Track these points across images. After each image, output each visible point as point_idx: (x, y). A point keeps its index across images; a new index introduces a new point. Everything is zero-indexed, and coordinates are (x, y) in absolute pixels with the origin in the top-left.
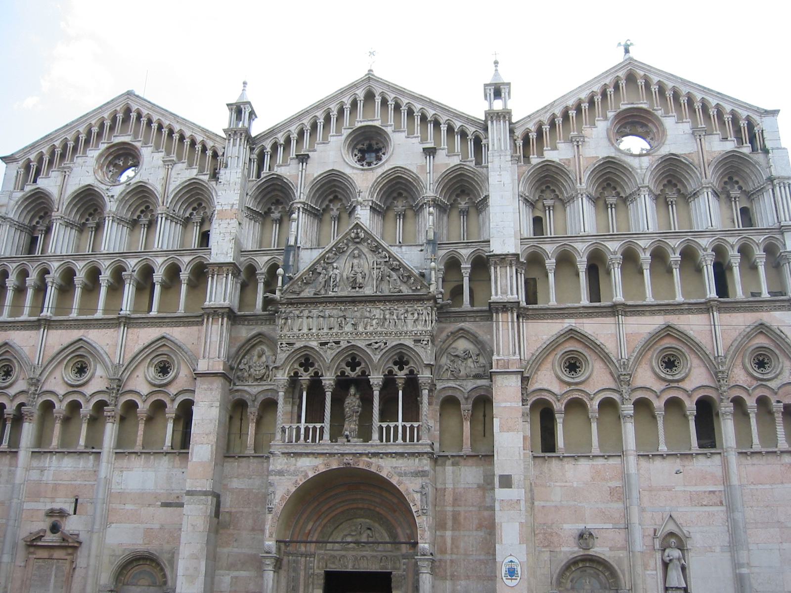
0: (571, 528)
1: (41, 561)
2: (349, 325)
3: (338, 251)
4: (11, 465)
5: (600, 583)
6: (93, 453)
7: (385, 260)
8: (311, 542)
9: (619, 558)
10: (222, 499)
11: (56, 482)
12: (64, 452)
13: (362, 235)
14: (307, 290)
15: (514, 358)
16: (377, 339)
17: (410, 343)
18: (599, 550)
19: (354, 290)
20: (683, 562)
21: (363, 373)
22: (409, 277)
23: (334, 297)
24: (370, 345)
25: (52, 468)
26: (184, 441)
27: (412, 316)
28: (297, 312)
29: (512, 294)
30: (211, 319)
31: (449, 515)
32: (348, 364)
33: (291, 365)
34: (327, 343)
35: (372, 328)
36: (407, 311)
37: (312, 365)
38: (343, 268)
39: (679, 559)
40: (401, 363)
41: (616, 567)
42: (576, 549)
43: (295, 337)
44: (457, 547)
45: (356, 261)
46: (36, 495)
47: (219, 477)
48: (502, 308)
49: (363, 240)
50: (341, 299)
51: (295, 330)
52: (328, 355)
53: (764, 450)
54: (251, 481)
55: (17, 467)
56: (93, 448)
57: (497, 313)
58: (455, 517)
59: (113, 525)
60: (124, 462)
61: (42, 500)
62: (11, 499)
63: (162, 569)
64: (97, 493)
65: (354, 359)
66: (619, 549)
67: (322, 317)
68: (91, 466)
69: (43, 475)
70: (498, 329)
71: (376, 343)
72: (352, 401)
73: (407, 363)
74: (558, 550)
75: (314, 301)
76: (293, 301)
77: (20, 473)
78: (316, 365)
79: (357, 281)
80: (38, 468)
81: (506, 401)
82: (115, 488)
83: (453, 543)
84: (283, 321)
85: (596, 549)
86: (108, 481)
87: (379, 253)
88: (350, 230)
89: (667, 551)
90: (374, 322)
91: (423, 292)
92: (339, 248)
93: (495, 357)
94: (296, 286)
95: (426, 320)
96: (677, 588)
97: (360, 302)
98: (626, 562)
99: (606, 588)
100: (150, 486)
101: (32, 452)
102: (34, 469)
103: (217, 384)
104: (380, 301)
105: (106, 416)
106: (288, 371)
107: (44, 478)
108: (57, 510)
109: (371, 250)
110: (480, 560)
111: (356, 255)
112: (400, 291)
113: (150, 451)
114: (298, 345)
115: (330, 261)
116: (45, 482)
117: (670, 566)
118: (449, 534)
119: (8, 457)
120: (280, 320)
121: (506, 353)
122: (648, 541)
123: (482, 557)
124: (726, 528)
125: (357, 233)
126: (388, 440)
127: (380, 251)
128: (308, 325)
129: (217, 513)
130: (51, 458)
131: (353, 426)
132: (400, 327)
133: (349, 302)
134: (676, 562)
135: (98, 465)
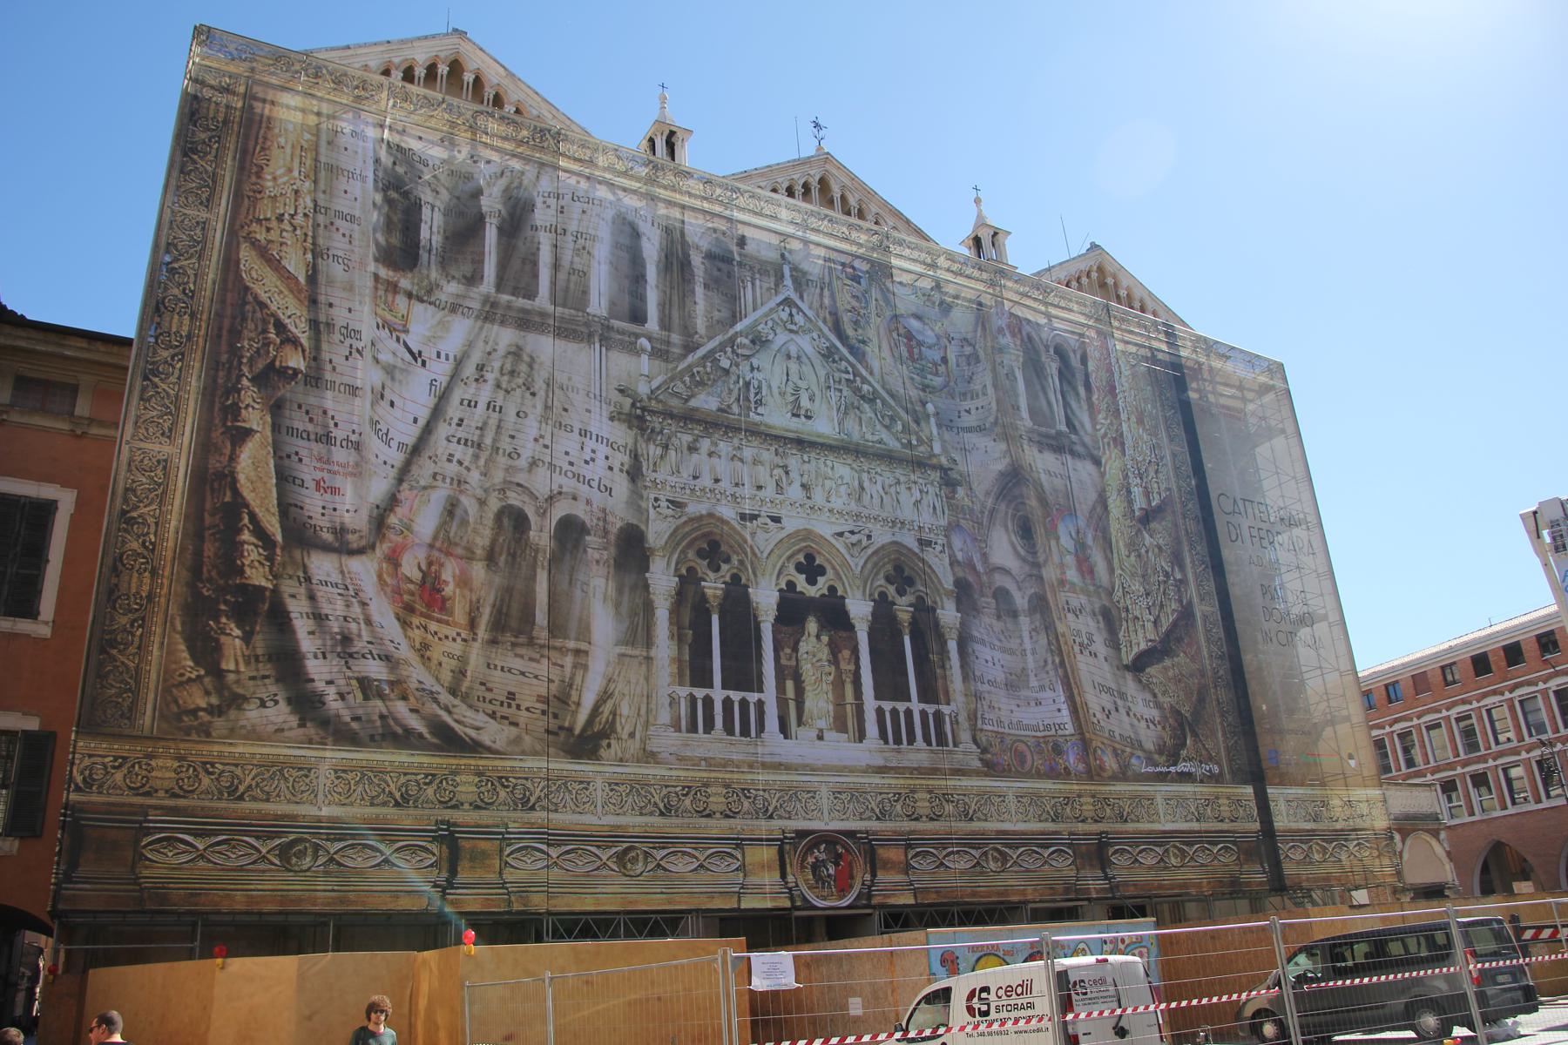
2: (797, 484)
7: (847, 376)
19: (795, 419)
22: (892, 418)
24: (841, 534)
28: (687, 439)
33: (683, 552)
34: (754, 517)
35: (840, 501)
36: (898, 483)
43: (688, 491)
51: (685, 475)
52: (764, 540)
65: (810, 558)
67: (741, 460)
71: (852, 533)
87: (834, 361)
95: (934, 508)
106: (677, 564)
114: (694, 509)
126: (898, 741)
127: (837, 358)
128: (713, 469)
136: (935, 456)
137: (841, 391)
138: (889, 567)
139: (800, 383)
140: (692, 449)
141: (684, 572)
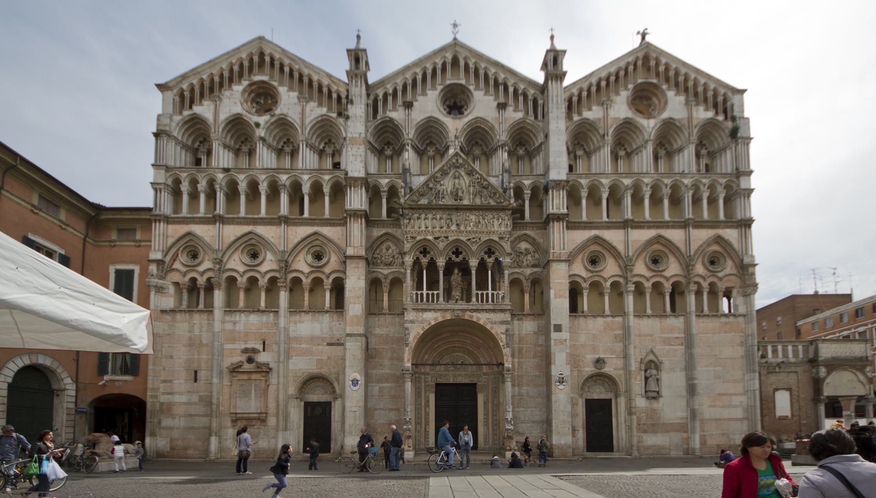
0: (590, 357)
3: (444, 173)
4: (208, 320)
5: (605, 388)
6: (272, 311)
8: (427, 365)
9: (619, 374)
10: (369, 340)
12: (249, 311)
13: (461, 161)
14: (422, 200)
15: (565, 251)
16: (474, 236)
17: (496, 239)
18: (608, 369)
20: (658, 377)
21: (464, 259)
22: (495, 194)
23: (443, 205)
24: (469, 239)
25: (241, 322)
26: (339, 303)
27: (497, 221)
29: (563, 209)
30: (352, 219)
31: (517, 349)
32: (453, 253)
36: (494, 218)
37: (429, 253)
38: (448, 184)
39: (655, 375)
40: (490, 252)
41: (617, 379)
42: (594, 369)
44: (522, 368)
45: (457, 181)
46: (233, 340)
47: (367, 327)
48: (557, 219)
49: (461, 166)
50: (447, 207)
51: (416, 228)
53: (711, 314)
54: (387, 329)
55: (214, 320)
56: (272, 308)
57: (553, 222)
58: (520, 351)
59: (294, 358)
61: (237, 342)
62: (213, 341)
63: (331, 384)
64: (280, 337)
65: (457, 249)
66: (619, 369)
67: (436, 219)
69: (236, 326)
70: (553, 233)
71: (474, 238)
72: (456, 277)
73: (493, 253)
74: (583, 369)
75: (428, 208)
76: (413, 207)
77: (217, 326)
78: (432, 253)
79: (459, 194)
80: (231, 322)
81: (558, 279)
82: (292, 334)
83: (518, 366)
84: (408, 221)
85: (605, 369)
86: (286, 330)
87: (473, 175)
88: (452, 157)
89: (648, 371)
90: (471, 224)
91: (505, 204)
92: (445, 170)
93: (552, 251)
94: (415, 196)
95: (507, 224)
96: (654, 391)
97: (462, 209)
98: (623, 377)
99: (608, 391)
100: (317, 333)
101: (225, 311)
102: (228, 322)
103: (362, 264)
104: (475, 209)
105: (279, 287)
107: (237, 328)
109: (467, 174)
110: (535, 375)
111: (457, 176)
112: (489, 203)
113: (316, 310)
115: (438, 180)
117: (650, 379)
118: (516, 360)
119: (206, 314)
120: (405, 220)
121: (558, 248)
122: (638, 365)
123: (537, 374)
124: (684, 358)
125: (457, 160)
128: (425, 224)
129: (367, 349)
131: (457, 293)
132: (489, 228)
133: (454, 209)
134: (654, 377)
135: (278, 319)
136: (511, 204)
137: (475, 186)
138: (486, 249)
139: (459, 187)
140: (418, 218)
141: (415, 259)
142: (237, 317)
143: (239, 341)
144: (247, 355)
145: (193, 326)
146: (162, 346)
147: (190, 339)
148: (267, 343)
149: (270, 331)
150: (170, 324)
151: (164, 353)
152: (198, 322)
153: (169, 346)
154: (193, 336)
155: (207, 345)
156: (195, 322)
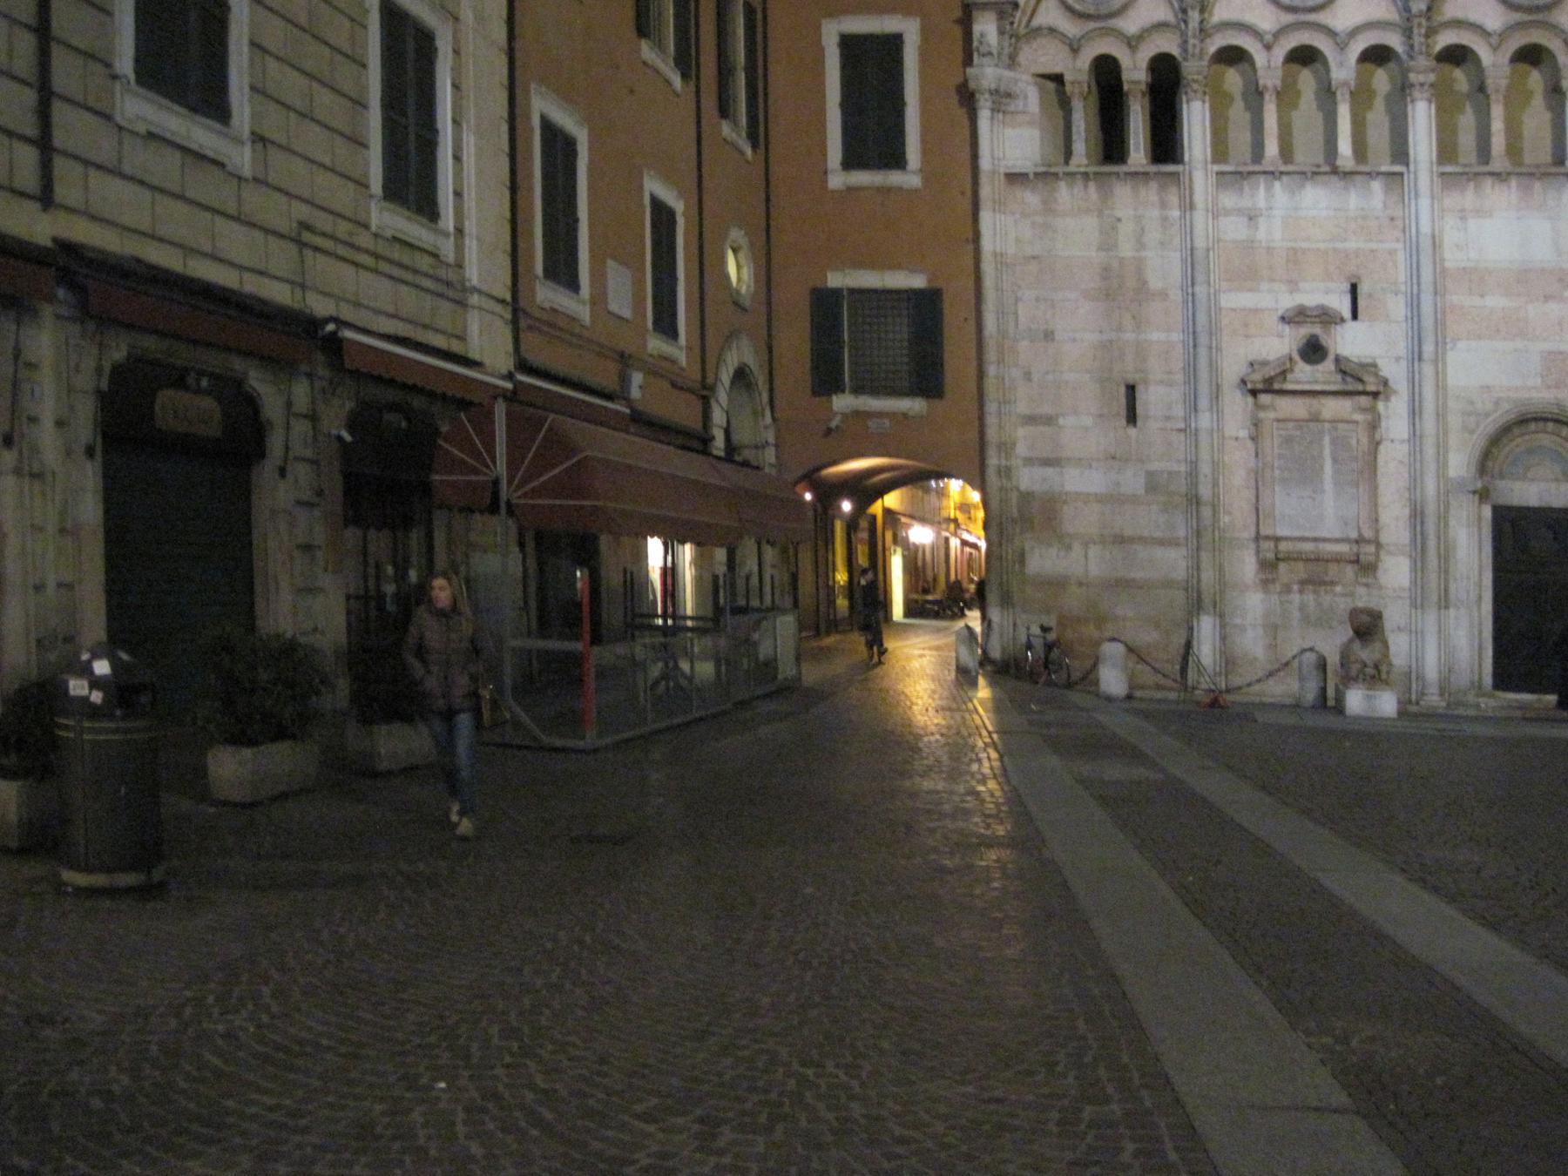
1: (1291, 425)
11: (1293, 245)
25: (1276, 212)
46: (1247, 276)
59: (1461, 345)
60: (1468, 198)
61: (1265, 286)
68: (1380, 206)
80: (1239, 211)
82: (1453, 258)
101: (1220, 174)
102: (1227, 213)
107: (1261, 234)
108: (1311, 309)
116: (1264, 244)
130: (1269, 189)
142: (1260, 195)
143: (1272, 280)
144: (1305, 331)
145: (1114, 228)
146: (1017, 300)
147: (1106, 271)
148: (1363, 290)
149: (1374, 246)
150: (1039, 219)
151: (1022, 319)
152: (1132, 212)
153: (1037, 300)
154: (1115, 264)
155: (1164, 295)
156: (1119, 214)
